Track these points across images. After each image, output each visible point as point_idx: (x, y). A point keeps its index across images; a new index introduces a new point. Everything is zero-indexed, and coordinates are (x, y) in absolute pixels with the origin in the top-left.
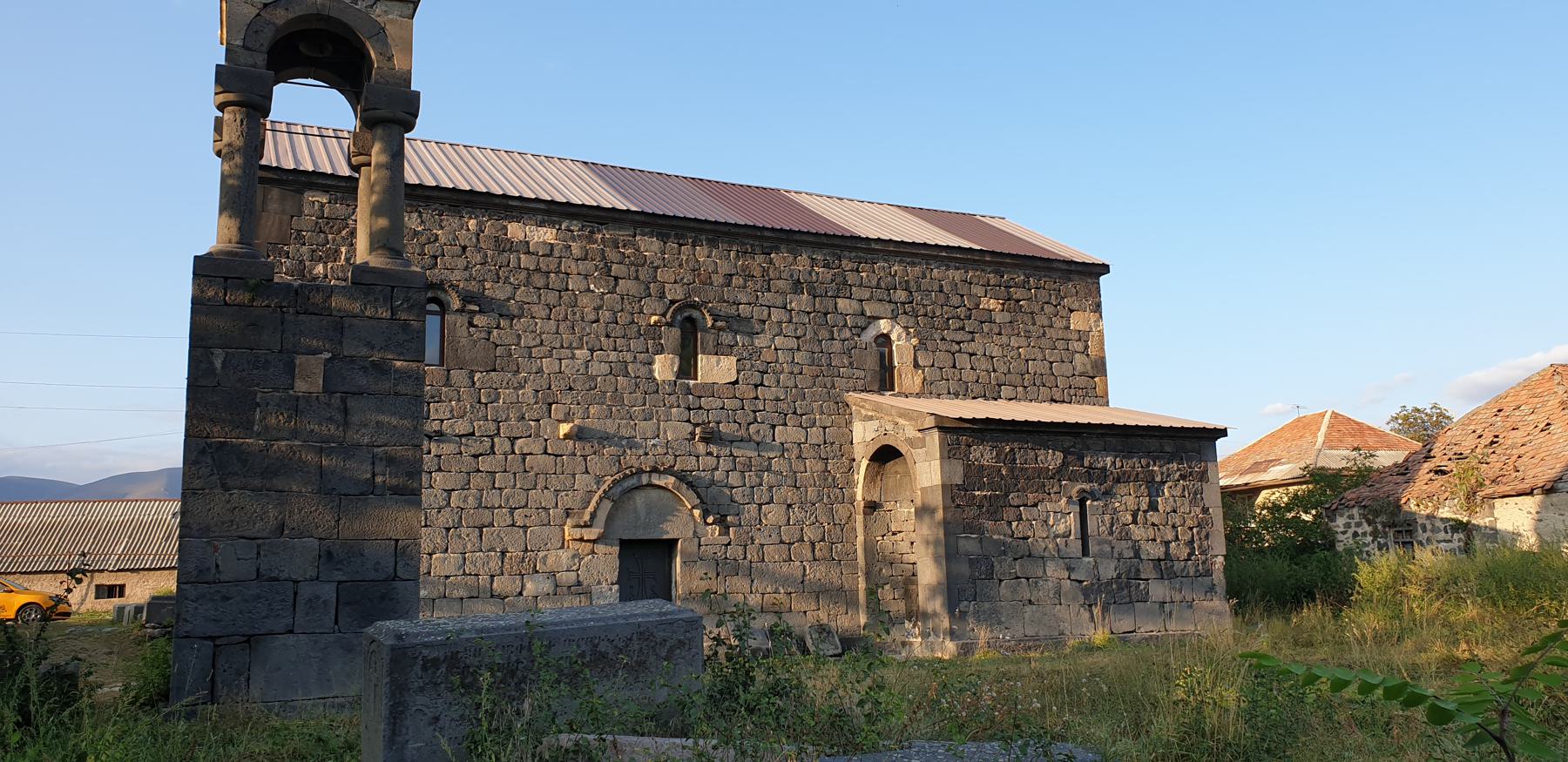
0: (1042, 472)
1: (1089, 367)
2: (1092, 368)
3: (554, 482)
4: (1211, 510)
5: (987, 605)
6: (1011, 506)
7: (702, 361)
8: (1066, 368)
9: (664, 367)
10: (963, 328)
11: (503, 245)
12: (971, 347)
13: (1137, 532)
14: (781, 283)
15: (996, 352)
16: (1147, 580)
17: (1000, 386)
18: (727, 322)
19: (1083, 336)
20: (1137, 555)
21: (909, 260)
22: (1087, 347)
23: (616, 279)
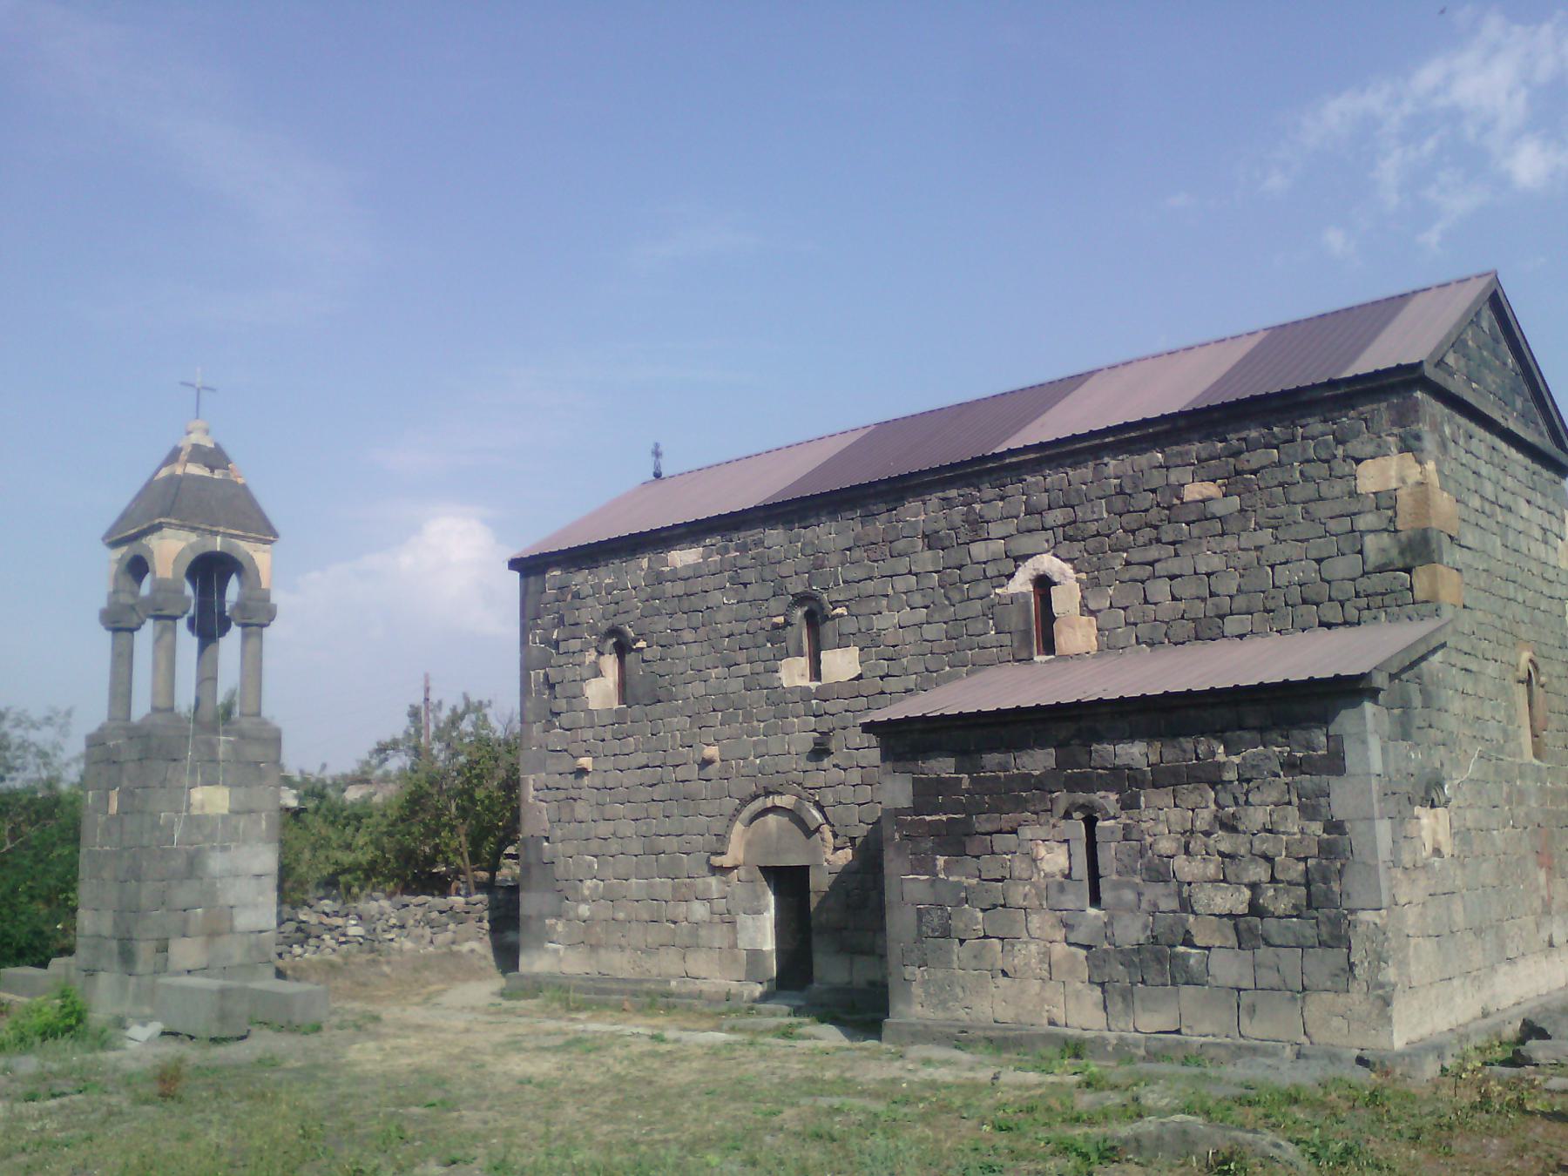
0: (1026, 781)
1: (1394, 553)
2: (1402, 553)
3: (706, 807)
4: (1348, 826)
5: (940, 974)
6: (977, 833)
7: (824, 655)
8: (1342, 567)
9: (793, 673)
10: (1158, 541)
11: (658, 578)
12: (1173, 566)
13: (1185, 867)
14: (900, 545)
15: (1217, 563)
16: (1208, 948)
17: (1222, 617)
18: (847, 607)
19: (1386, 501)
20: (1186, 905)
21: (1069, 461)
22: (1391, 520)
23: (745, 585)
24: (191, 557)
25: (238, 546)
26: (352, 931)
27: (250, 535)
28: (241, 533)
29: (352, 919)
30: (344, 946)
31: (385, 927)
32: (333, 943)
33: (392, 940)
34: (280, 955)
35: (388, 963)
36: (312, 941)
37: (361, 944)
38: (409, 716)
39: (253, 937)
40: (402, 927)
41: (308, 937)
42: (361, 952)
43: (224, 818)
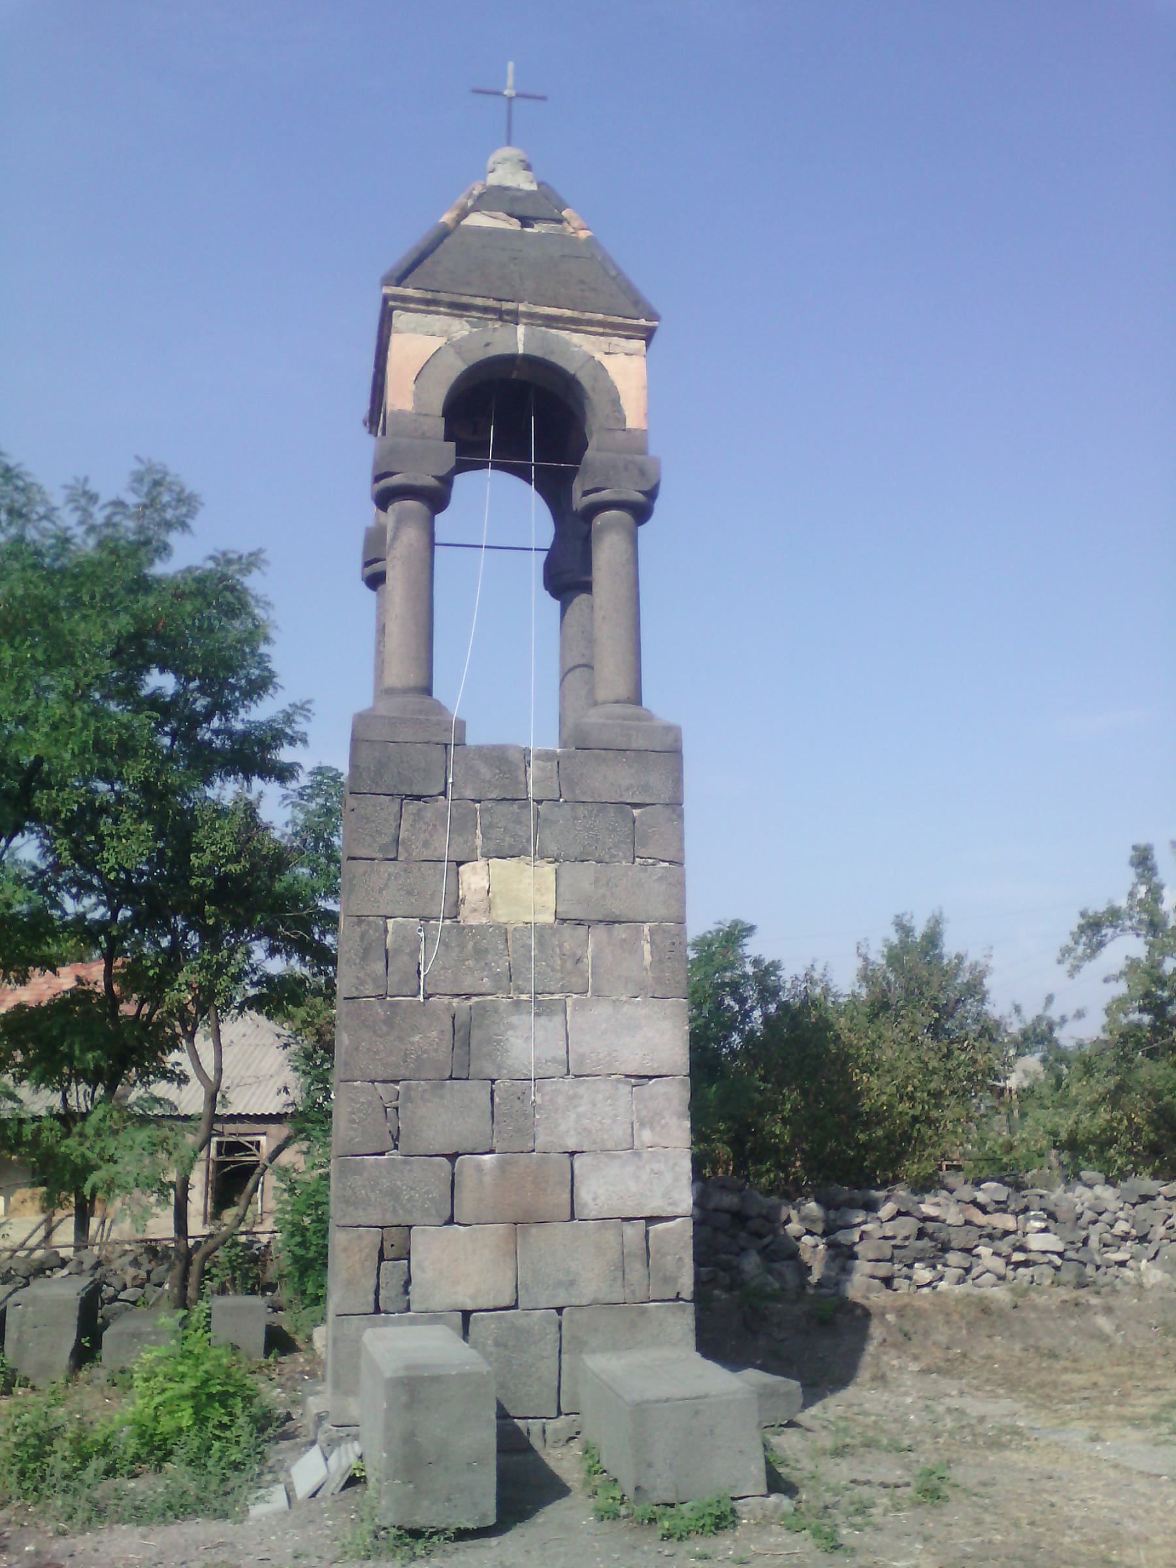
24: (457, 367)
25: (568, 343)
26: (1036, 1242)
27: (588, 316)
28: (567, 313)
29: (1036, 1218)
30: (1021, 1270)
31: (1108, 1237)
32: (998, 1264)
33: (1122, 1264)
34: (887, 1281)
35: (1108, 1310)
36: (953, 1258)
37: (1057, 1268)
38: (1132, 864)
39: (633, 1232)
40: (1143, 1239)
41: (945, 1248)
42: (1056, 1283)
43: (542, 931)
